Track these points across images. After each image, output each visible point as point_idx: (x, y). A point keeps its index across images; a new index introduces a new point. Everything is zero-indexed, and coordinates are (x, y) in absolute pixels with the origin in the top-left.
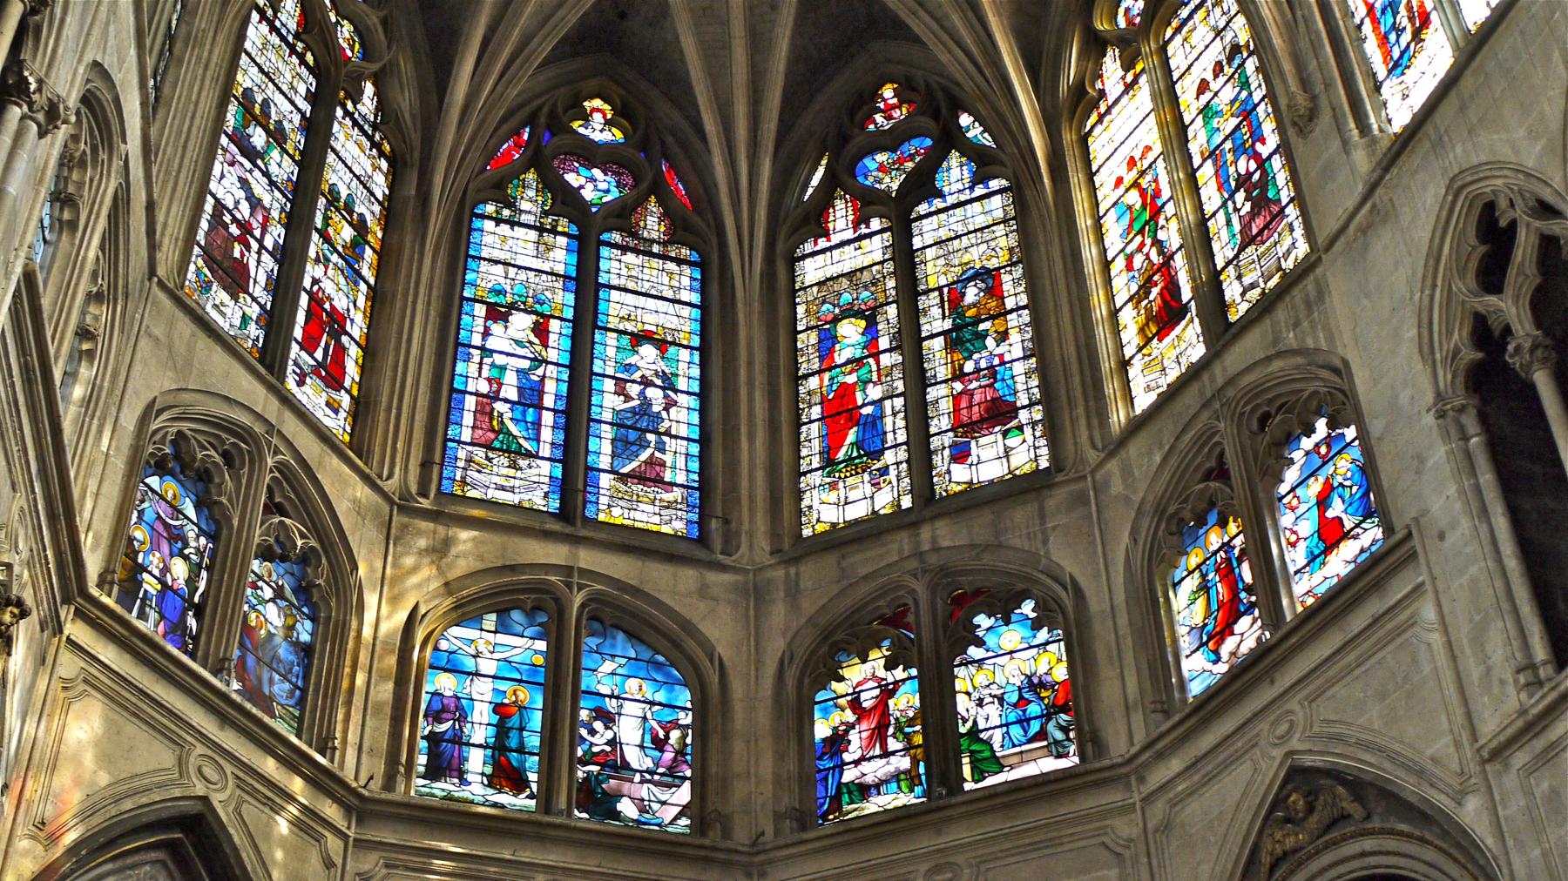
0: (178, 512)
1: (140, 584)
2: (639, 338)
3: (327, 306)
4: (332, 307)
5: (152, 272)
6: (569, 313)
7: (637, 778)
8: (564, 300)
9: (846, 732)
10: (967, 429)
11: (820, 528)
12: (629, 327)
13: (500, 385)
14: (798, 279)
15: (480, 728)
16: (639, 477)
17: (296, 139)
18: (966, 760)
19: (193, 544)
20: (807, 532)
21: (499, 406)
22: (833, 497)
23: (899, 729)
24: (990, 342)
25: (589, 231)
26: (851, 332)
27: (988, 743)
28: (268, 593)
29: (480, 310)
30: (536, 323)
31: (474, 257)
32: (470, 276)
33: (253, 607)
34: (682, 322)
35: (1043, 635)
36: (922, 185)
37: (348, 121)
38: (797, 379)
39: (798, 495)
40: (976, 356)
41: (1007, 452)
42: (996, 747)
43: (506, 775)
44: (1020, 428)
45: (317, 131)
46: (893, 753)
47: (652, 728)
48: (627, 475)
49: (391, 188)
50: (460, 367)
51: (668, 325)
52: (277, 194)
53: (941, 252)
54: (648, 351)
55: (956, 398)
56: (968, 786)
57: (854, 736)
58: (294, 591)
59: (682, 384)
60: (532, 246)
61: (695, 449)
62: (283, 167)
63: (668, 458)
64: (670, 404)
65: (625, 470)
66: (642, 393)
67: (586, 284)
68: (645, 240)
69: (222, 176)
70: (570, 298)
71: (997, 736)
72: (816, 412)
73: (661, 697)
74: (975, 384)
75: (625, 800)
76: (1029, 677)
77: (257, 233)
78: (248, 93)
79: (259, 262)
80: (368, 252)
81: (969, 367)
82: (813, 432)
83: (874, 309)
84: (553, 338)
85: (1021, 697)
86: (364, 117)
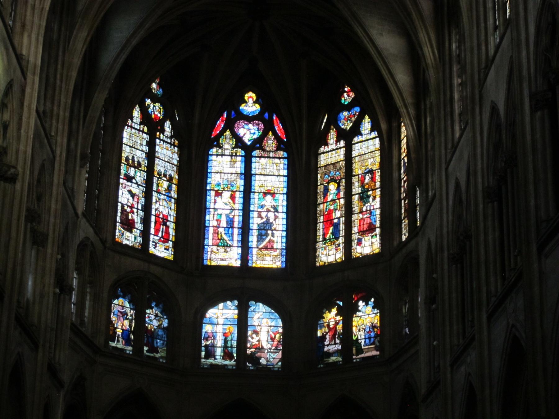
0: (123, 307)
1: (116, 333)
2: (265, 194)
3: (161, 216)
4: (163, 215)
5: (105, 247)
6: (242, 189)
7: (266, 351)
8: (240, 183)
9: (326, 335)
10: (362, 233)
11: (322, 264)
12: (263, 190)
13: (220, 221)
14: (319, 163)
15: (219, 342)
16: (266, 248)
17: (144, 163)
18: (354, 349)
19: (129, 314)
20: (318, 264)
21: (221, 230)
22: (325, 253)
23: (339, 336)
24: (371, 199)
25: (249, 151)
26: (333, 187)
27: (360, 344)
28: (153, 317)
29: (213, 193)
30: (232, 195)
31: (210, 172)
32: (209, 180)
33: (149, 324)
34: (280, 184)
35: (376, 311)
36: (356, 130)
37: (162, 142)
38: (316, 205)
39: (315, 250)
40: (367, 205)
41: (372, 243)
42: (362, 345)
43: (227, 355)
44: (376, 235)
45: (151, 156)
46: (337, 344)
47: (271, 335)
48: (262, 248)
49: (179, 157)
50: (207, 217)
51: (275, 186)
52: (141, 187)
53: (360, 160)
54: (269, 197)
55: (360, 220)
56: (354, 357)
57: (327, 336)
58: (161, 313)
59: (280, 209)
60: (229, 163)
61: (284, 234)
62: (140, 176)
63: (275, 239)
64: (276, 218)
65: (261, 247)
66: (267, 215)
67: (248, 176)
68: (268, 151)
69: (123, 193)
70: (242, 181)
71: (363, 341)
72: (322, 218)
73: (273, 324)
74: (365, 216)
75: (262, 359)
76: (372, 324)
77: (136, 206)
78: (127, 159)
79: (137, 215)
80: (174, 186)
81: (364, 209)
82: (320, 226)
83: (340, 180)
84: (237, 200)
85: (370, 330)
86: (167, 137)
